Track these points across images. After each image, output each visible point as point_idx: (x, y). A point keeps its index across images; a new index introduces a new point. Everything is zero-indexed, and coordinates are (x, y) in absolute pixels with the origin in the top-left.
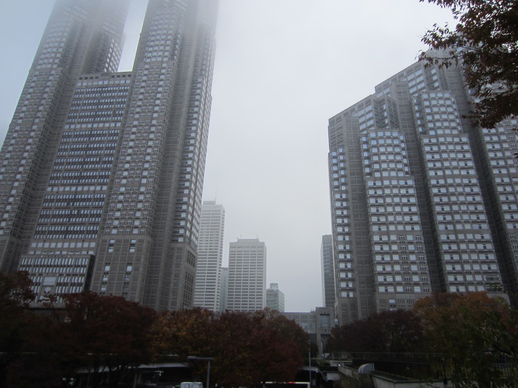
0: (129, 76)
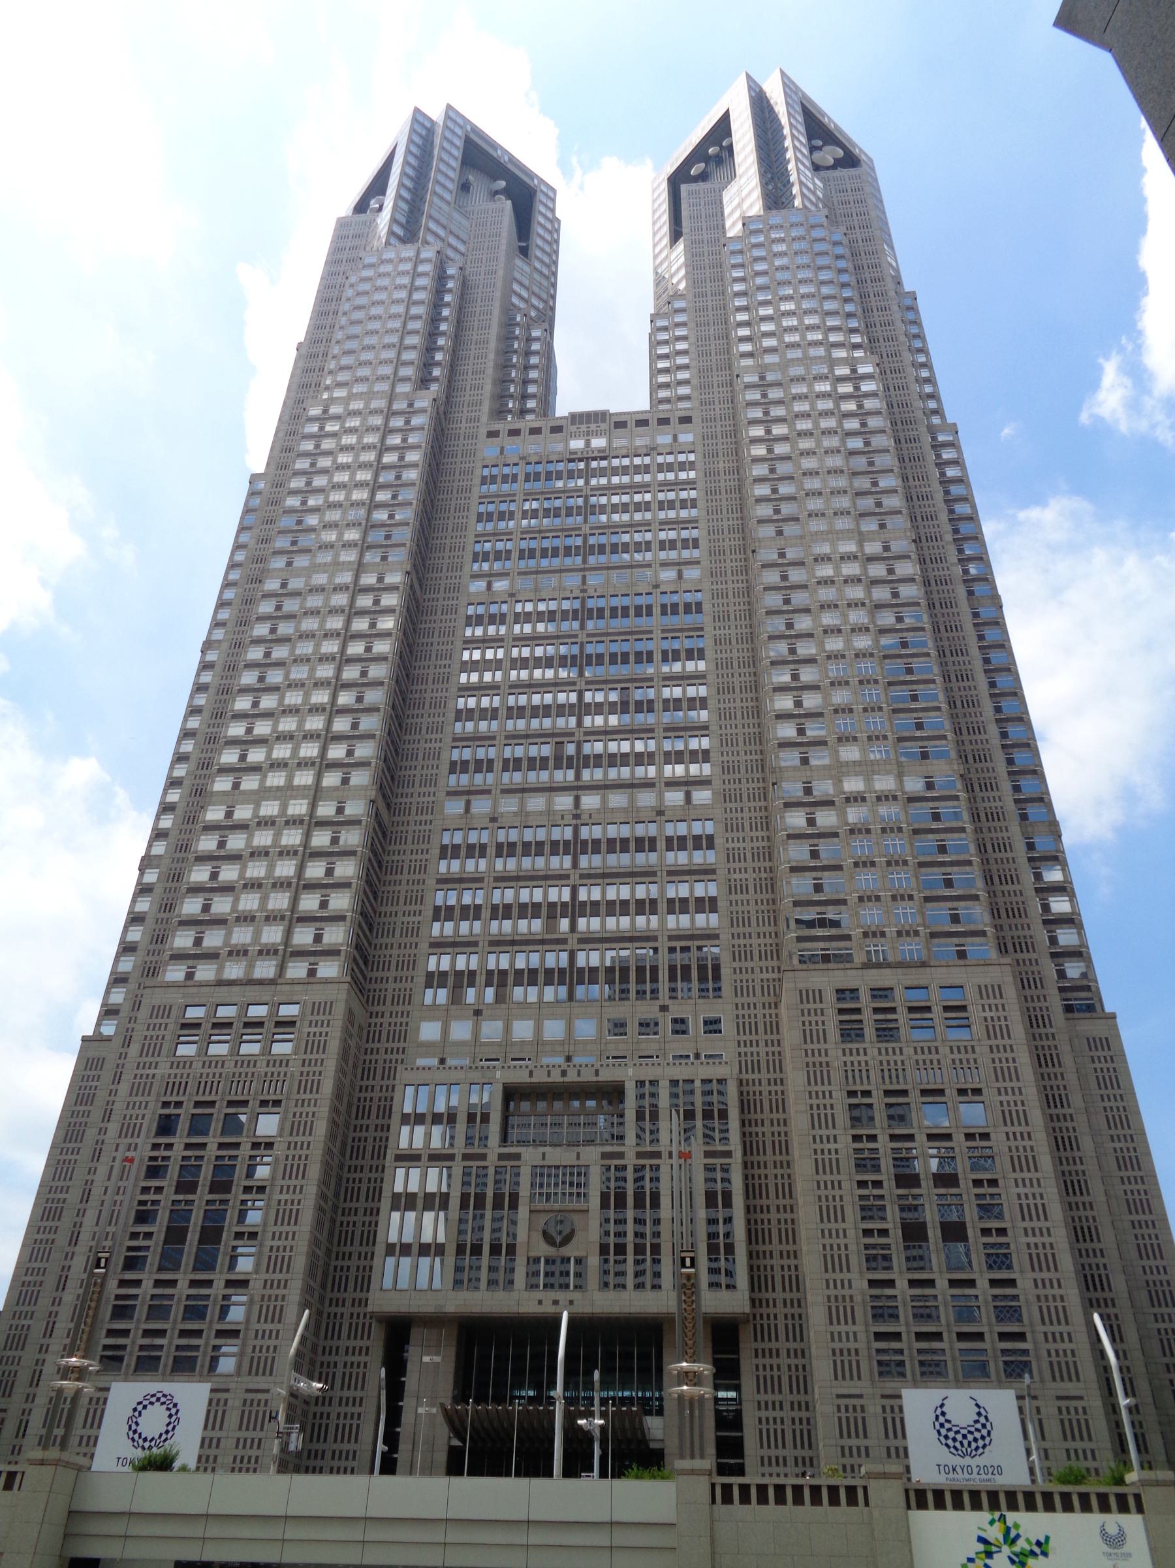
0: (686, 420)
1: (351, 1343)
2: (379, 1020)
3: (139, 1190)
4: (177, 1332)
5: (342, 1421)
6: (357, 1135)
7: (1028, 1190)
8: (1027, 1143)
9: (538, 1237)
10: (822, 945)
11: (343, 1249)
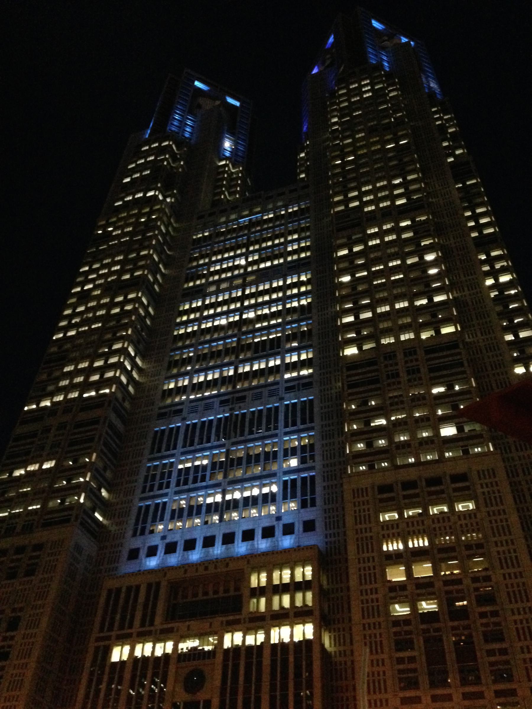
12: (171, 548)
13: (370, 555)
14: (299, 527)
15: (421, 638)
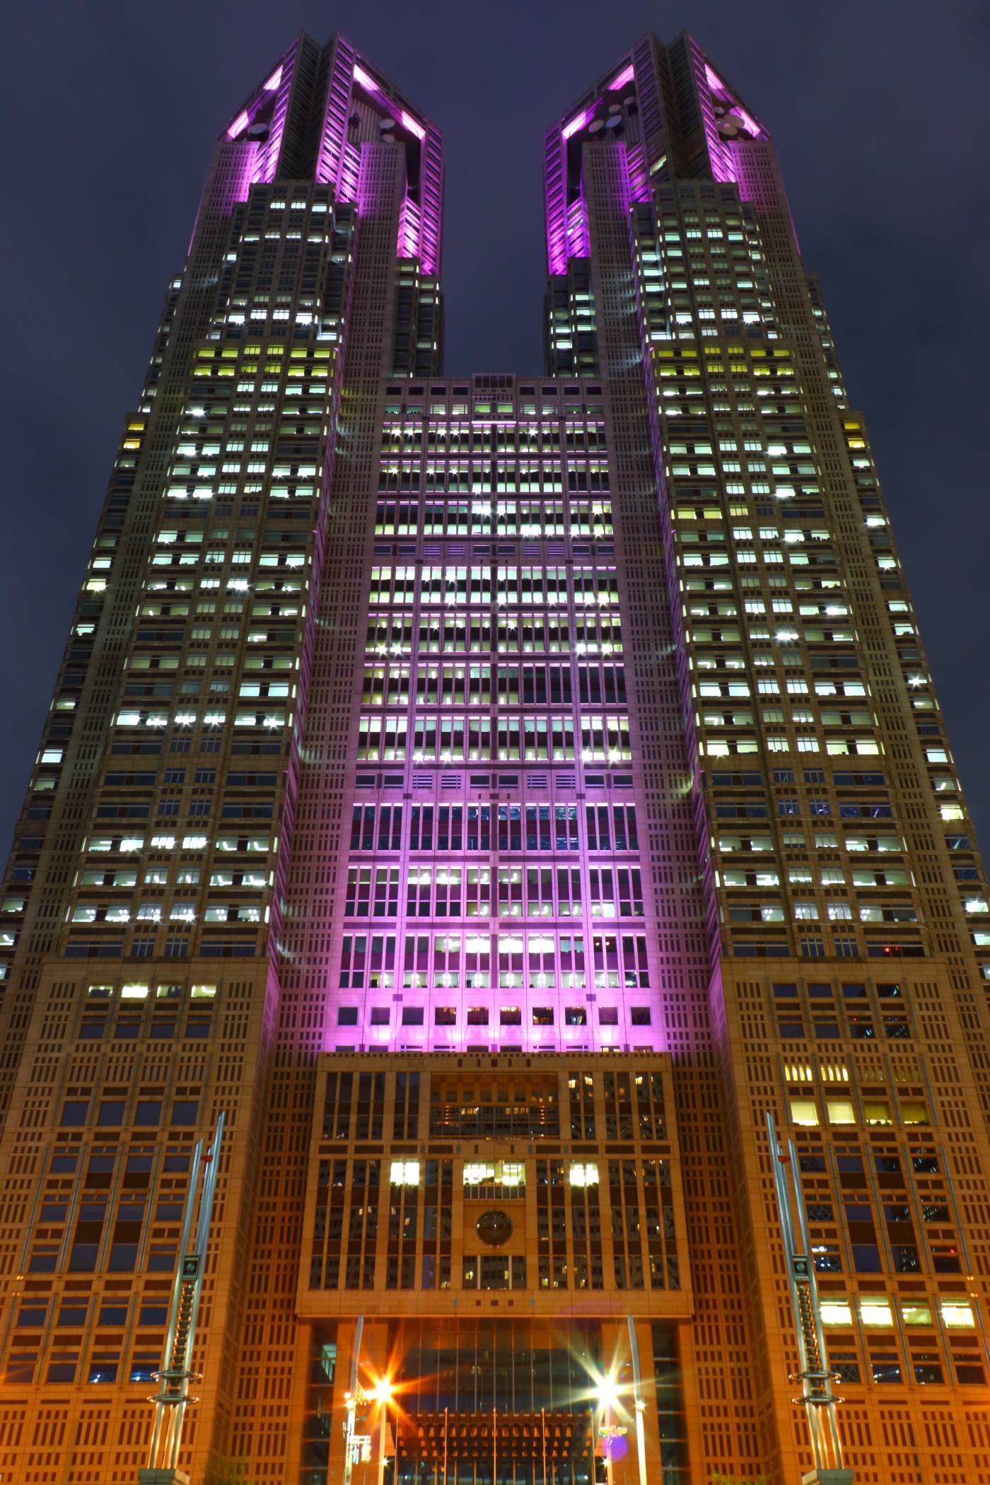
0: (595, 391)
1: (274, 1348)
2: (293, 1003)
3: (45, 1184)
4: (133, 1339)
5: (266, 1432)
6: (274, 1124)
7: (971, 1192)
8: (969, 1144)
9: (473, 1234)
10: (756, 938)
11: (261, 1247)
12: (413, 1017)
13: (768, 1084)
14: (624, 1016)
15: (843, 1208)
